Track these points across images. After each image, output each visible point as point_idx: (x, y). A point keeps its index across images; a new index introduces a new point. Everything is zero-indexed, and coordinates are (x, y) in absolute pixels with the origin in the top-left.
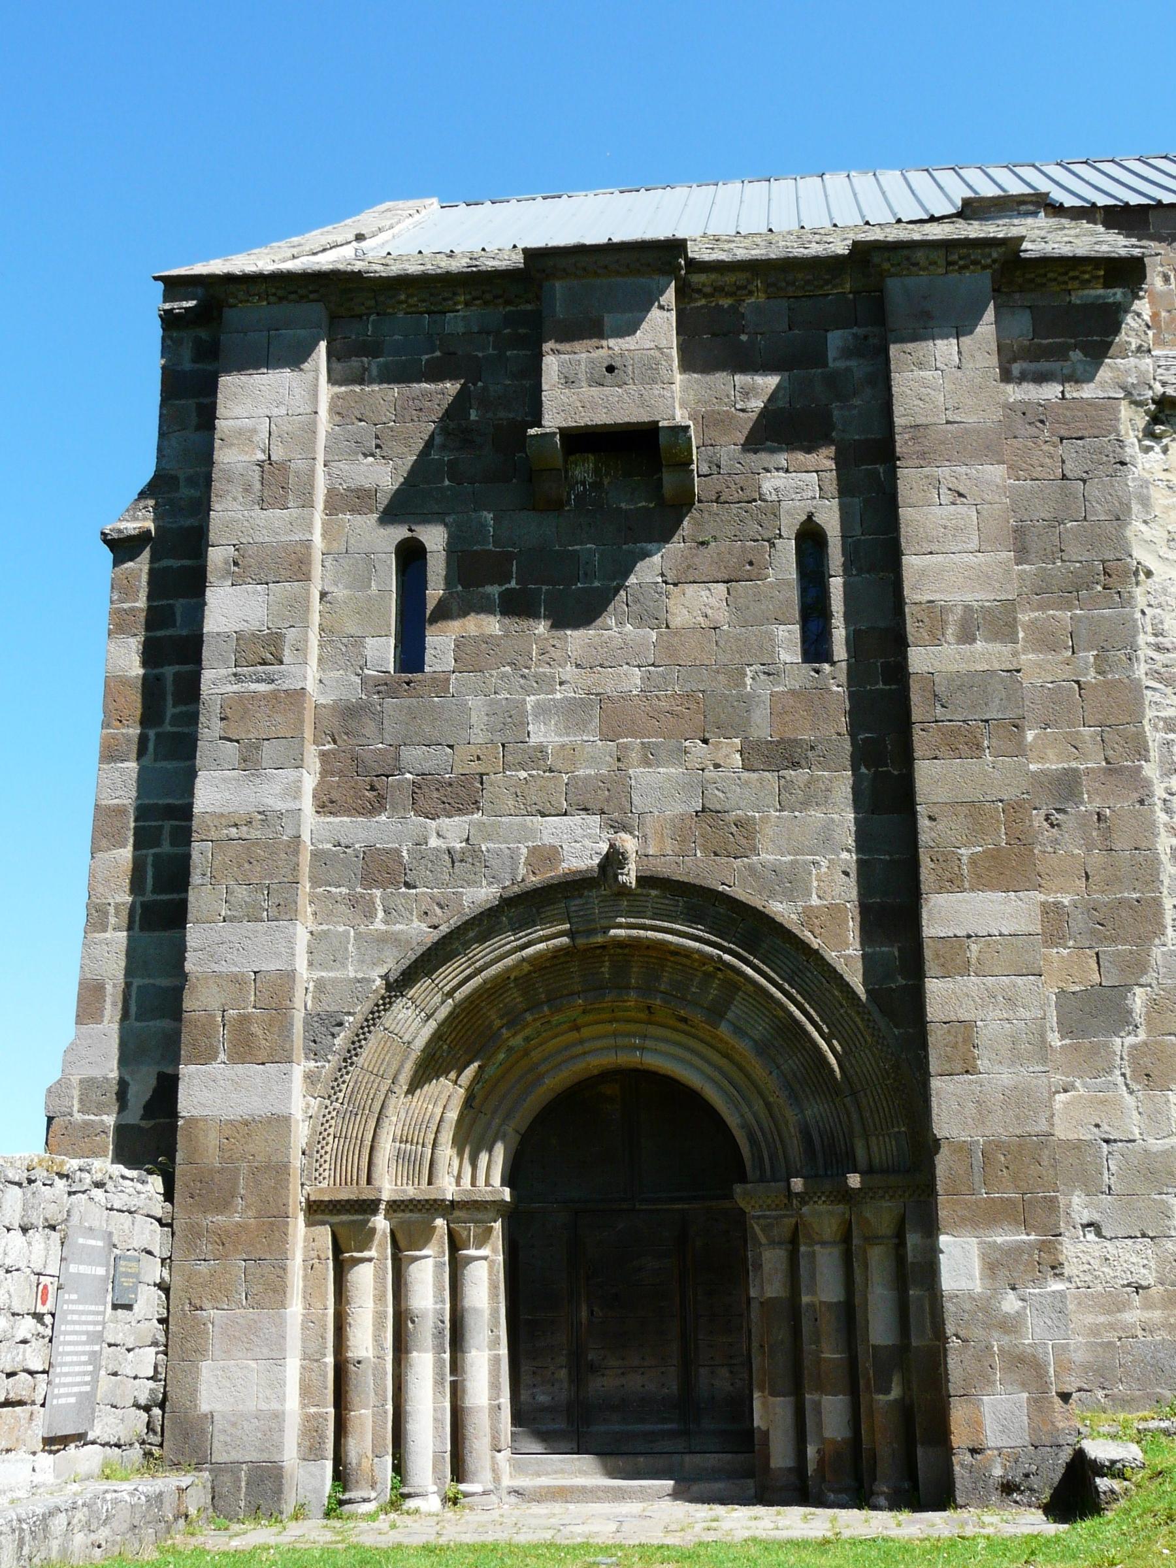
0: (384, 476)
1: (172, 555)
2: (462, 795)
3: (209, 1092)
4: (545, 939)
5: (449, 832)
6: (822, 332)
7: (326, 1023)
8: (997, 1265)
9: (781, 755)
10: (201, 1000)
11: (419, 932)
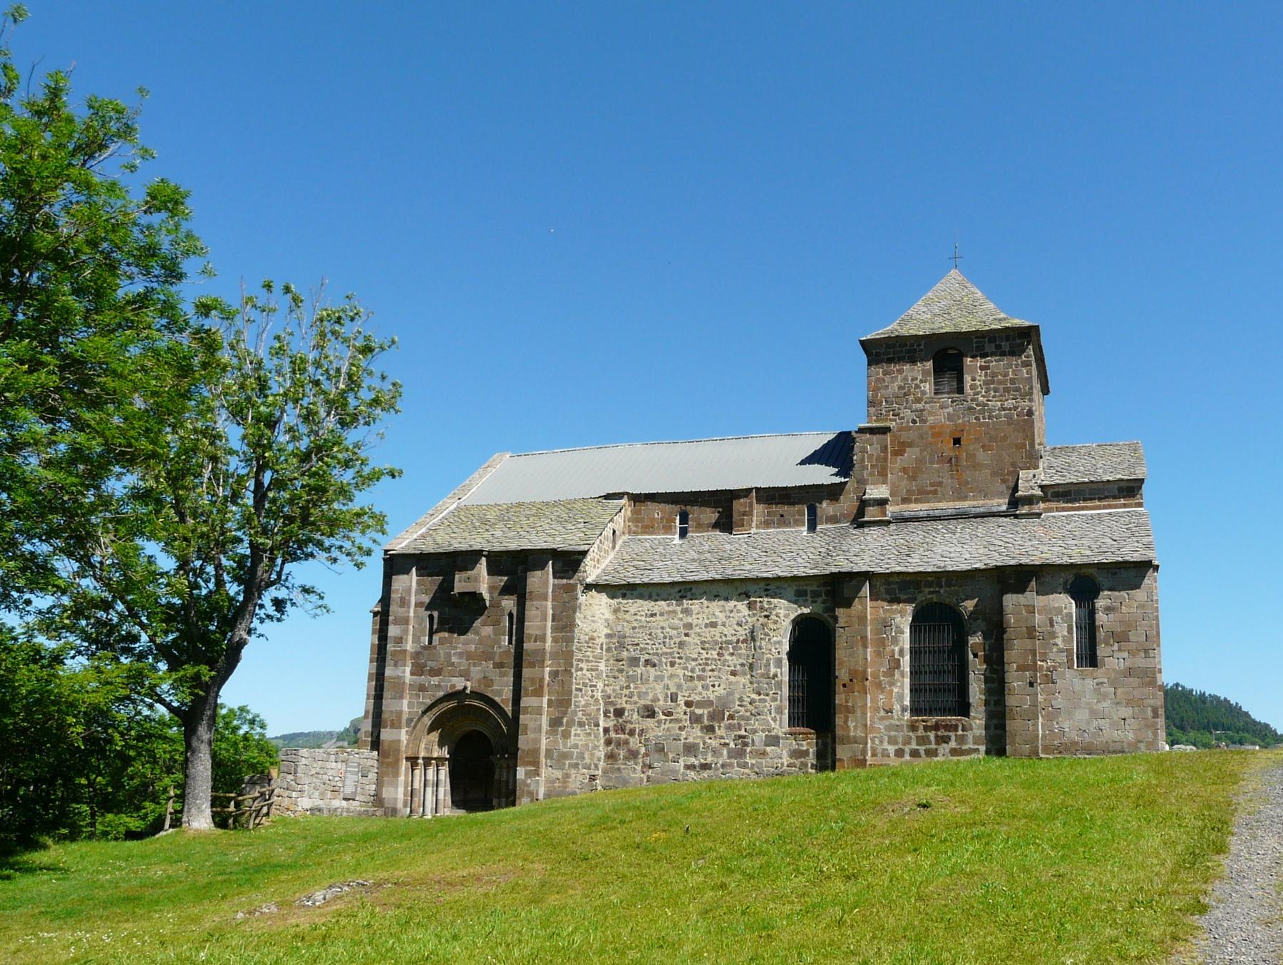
0: (426, 599)
1: (383, 616)
2: (436, 672)
3: (386, 734)
4: (452, 704)
5: (435, 680)
6: (515, 567)
7: (409, 721)
8: (528, 774)
9: (499, 665)
10: (384, 716)
11: (429, 702)
